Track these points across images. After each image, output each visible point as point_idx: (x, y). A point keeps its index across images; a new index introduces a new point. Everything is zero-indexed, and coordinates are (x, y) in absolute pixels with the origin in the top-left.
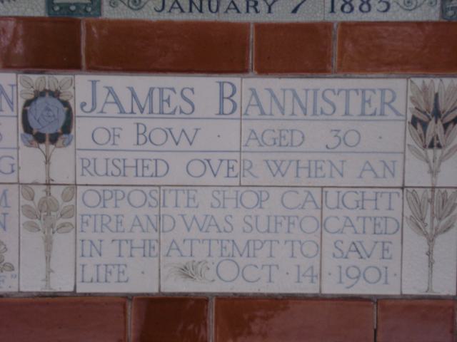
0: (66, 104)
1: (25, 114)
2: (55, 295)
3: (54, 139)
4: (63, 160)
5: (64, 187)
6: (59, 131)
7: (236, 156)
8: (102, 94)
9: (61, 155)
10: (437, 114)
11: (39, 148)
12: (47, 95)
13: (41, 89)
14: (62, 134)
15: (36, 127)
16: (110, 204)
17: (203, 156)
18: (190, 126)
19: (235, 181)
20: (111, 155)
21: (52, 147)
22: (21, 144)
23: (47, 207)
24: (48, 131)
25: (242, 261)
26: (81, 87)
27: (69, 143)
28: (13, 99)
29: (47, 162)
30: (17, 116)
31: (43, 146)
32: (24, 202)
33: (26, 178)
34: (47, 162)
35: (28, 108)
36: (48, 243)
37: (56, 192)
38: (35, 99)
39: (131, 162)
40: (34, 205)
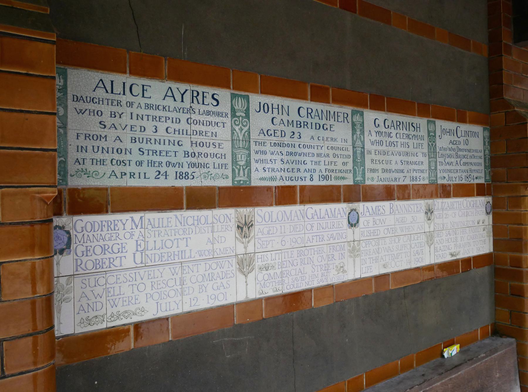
2: (356, 280)
7: (393, 227)
8: (365, 208)
9: (357, 230)
10: (429, 210)
16: (368, 246)
17: (387, 227)
18: (384, 217)
19: (393, 235)
20: (368, 229)
23: (354, 249)
24: (354, 223)
25: (396, 260)
26: (361, 206)
32: (349, 248)
36: (354, 261)
39: (372, 231)
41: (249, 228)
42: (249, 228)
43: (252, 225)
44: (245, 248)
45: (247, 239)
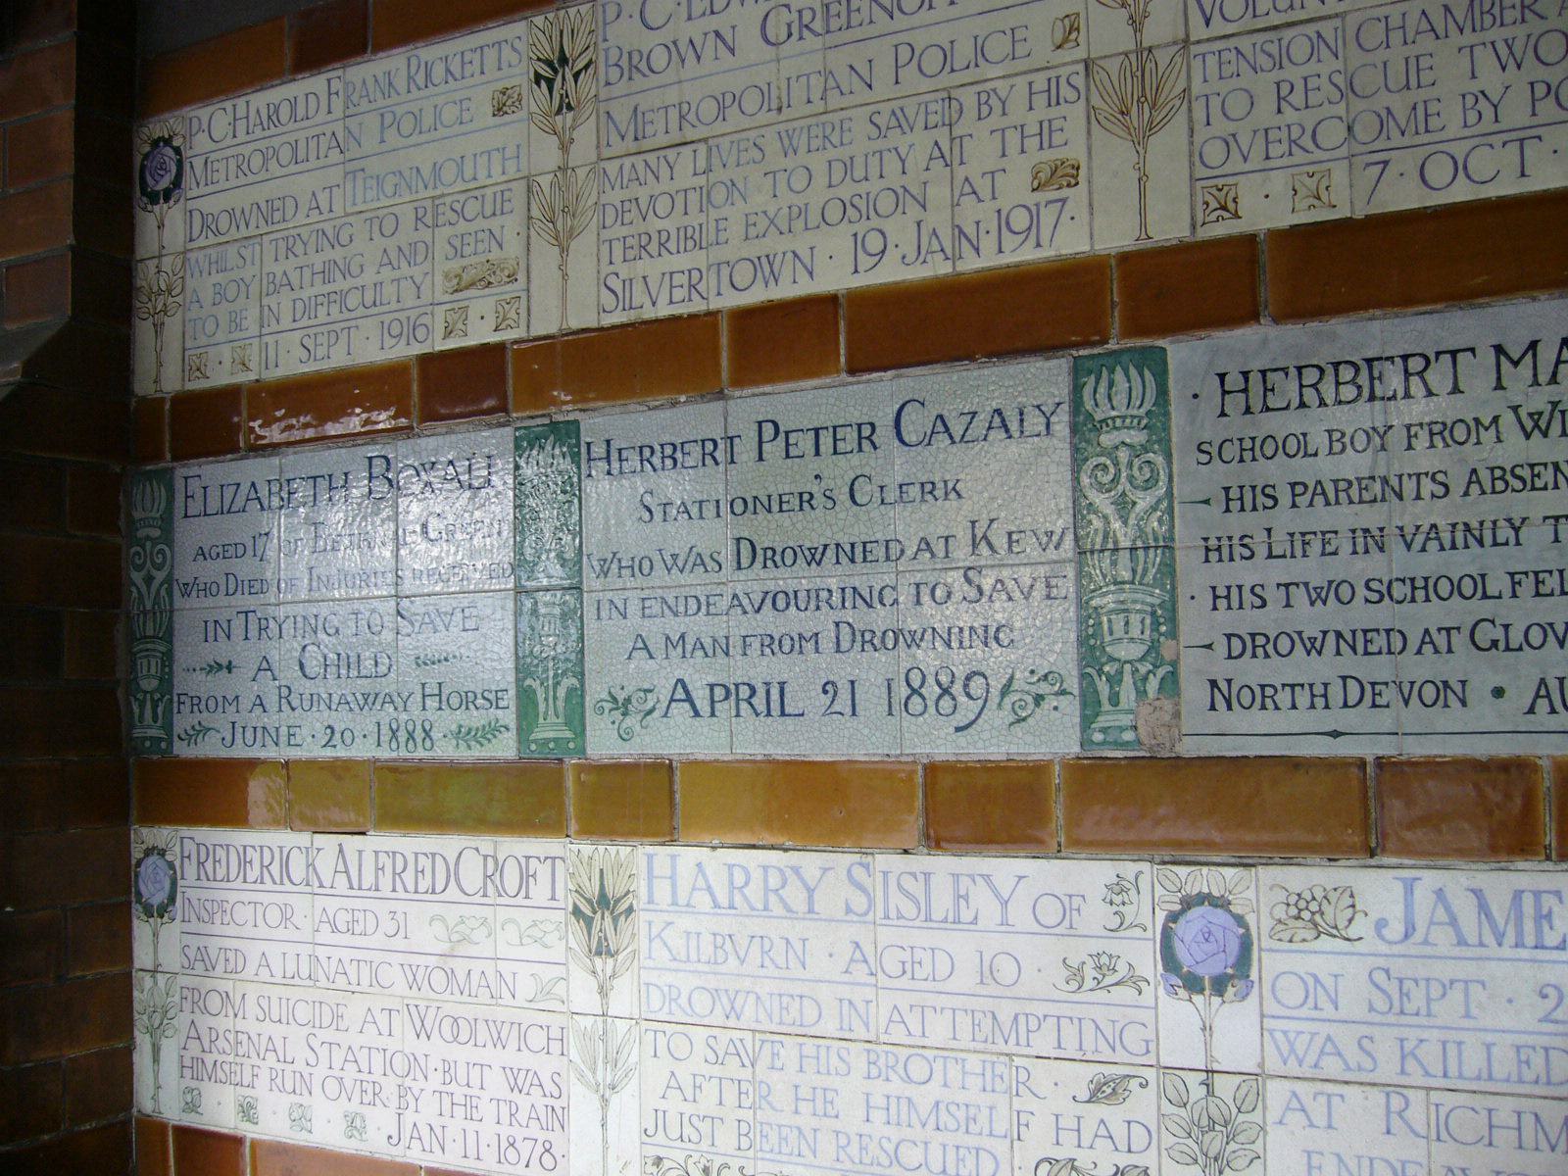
0: (1240, 920)
1: (1167, 936)
3: (1219, 985)
4: (1235, 1031)
5: (1238, 1079)
11: (1190, 1000)
22: (1161, 991)
24: (1206, 972)
29: (1207, 1028)
31: (1198, 999)
37: (1224, 1086)
38: (1183, 912)
41: (615, 920)
42: (615, 920)
43: (630, 910)
44: (603, 992)
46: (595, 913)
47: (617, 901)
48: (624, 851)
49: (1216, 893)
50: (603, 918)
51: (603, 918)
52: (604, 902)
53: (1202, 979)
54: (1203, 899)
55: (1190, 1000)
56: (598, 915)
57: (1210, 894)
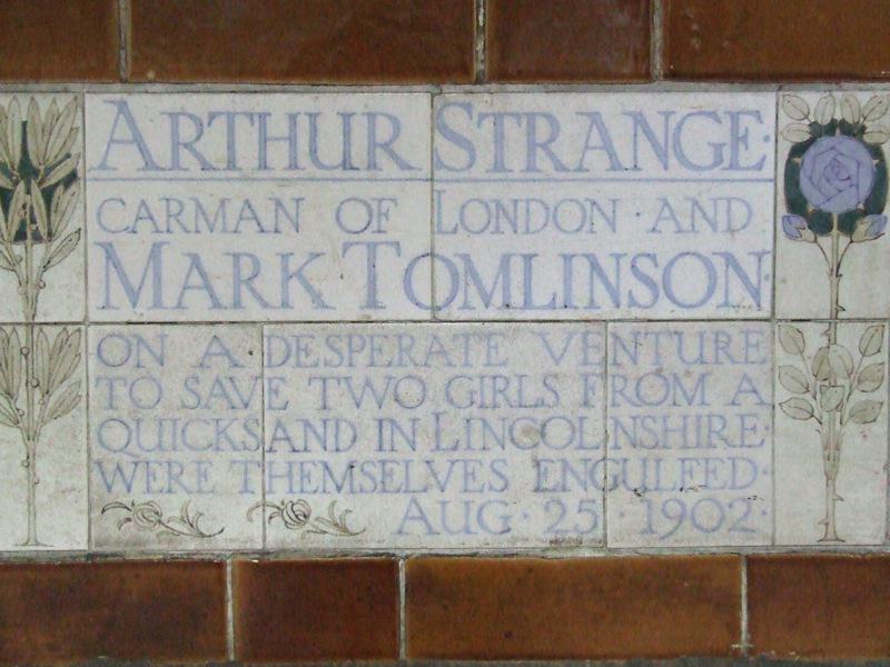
1: (792, 174)
3: (848, 223)
6: (861, 206)
12: (838, 131)
13: (826, 121)
14: (865, 213)
15: (815, 200)
21: (844, 240)
22: (781, 234)
27: (878, 235)
28: (666, 146)
29: (836, 272)
30: (775, 180)
31: (825, 241)
33: (790, 306)
34: (836, 272)
35: (797, 160)
37: (848, 336)
40: (804, 367)
41: (48, 195)
42: (48, 195)
43: (72, 178)
45: (39, 250)
46: (16, 183)
47: (49, 170)
48: (63, 101)
49: (849, 120)
50: (28, 192)
51: (28, 192)
52: (27, 170)
53: (830, 214)
54: (832, 128)
55: (815, 241)
56: (21, 186)
57: (843, 122)
